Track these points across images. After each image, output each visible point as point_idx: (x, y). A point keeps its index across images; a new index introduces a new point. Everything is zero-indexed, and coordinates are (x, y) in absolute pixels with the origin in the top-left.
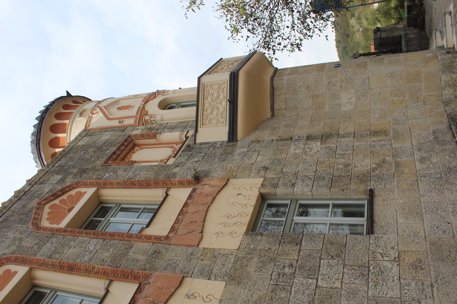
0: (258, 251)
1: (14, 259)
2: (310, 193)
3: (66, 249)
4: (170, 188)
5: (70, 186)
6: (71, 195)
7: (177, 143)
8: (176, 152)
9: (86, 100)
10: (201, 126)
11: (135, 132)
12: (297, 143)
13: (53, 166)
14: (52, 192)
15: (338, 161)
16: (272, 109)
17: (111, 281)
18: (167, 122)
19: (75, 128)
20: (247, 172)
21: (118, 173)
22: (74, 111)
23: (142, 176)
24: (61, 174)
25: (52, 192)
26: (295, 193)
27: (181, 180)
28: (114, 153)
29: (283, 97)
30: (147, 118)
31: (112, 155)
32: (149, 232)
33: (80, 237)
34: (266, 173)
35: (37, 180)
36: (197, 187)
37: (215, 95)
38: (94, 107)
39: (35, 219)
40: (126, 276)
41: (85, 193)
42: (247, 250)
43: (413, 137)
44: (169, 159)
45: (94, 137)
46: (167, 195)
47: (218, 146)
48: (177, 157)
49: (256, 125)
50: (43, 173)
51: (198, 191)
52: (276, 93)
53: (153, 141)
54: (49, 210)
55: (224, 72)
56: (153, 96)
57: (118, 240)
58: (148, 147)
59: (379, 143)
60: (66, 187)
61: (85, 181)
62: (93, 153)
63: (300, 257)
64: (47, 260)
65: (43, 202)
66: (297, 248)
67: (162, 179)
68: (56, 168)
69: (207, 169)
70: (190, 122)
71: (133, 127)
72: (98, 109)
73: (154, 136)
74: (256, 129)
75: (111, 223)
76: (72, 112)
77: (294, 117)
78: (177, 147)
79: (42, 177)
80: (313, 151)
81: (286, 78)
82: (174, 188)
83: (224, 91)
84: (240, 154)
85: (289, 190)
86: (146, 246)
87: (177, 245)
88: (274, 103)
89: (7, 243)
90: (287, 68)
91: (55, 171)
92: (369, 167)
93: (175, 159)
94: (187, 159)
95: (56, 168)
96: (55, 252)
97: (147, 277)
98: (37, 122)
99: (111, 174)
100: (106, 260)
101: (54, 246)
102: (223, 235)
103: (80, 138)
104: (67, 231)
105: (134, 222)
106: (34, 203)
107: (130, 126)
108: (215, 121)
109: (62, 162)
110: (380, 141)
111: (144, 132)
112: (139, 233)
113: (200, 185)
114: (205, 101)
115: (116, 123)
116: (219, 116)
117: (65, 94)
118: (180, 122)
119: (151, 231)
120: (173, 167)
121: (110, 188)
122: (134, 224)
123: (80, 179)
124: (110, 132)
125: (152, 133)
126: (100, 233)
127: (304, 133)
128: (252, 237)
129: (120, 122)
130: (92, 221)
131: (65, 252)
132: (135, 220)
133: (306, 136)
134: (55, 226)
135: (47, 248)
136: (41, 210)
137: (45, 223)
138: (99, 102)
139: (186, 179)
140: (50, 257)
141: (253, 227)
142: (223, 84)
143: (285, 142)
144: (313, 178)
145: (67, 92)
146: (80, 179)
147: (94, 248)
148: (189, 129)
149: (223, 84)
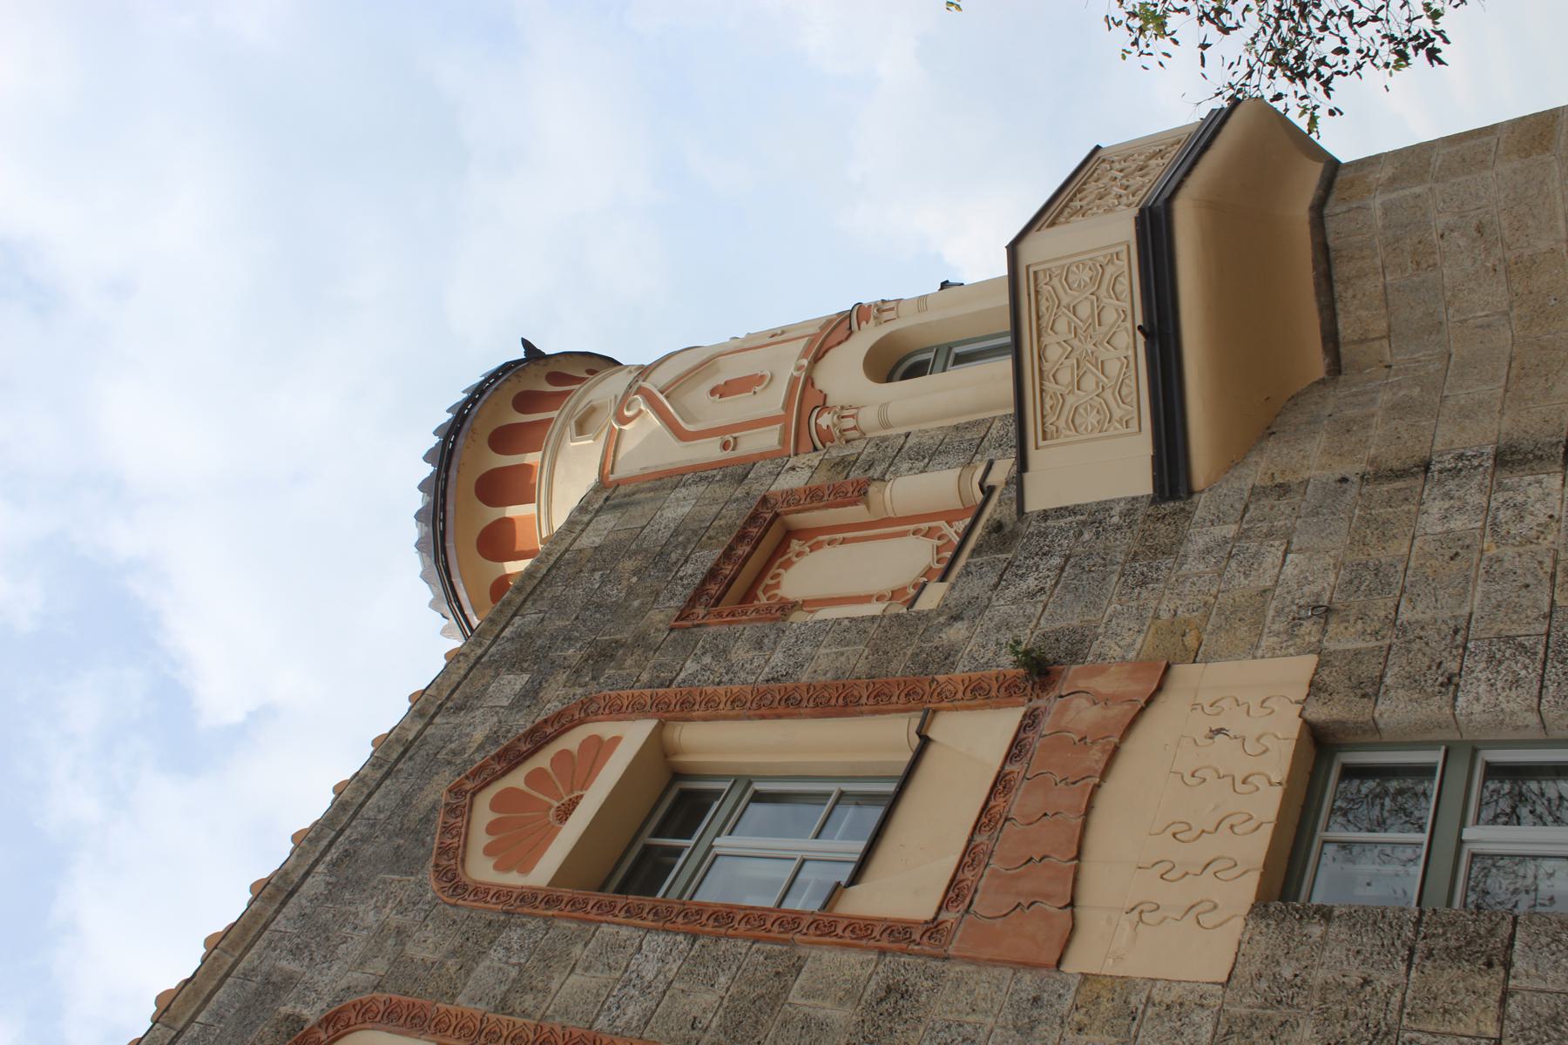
0: (1317, 994)
1: (382, 1008)
2: (1533, 719)
3: (556, 975)
4: (935, 711)
5: (559, 715)
6: (565, 753)
7: (950, 516)
8: (948, 554)
9: (599, 364)
10: (1041, 443)
12: (1451, 485)
13: (497, 637)
14: (496, 742)
16: (1331, 339)
18: (903, 430)
19: (566, 478)
20: (1243, 631)
21: (733, 657)
22: (554, 414)
23: (823, 664)
24: (523, 671)
25: (496, 742)
26: (1461, 719)
27: (975, 675)
28: (712, 574)
30: (826, 420)
31: (703, 582)
32: (863, 902)
33: (604, 928)
34: (1324, 631)
35: (445, 694)
36: (1041, 703)
37: (1084, 310)
38: (626, 394)
39: (444, 850)
41: (616, 740)
42: (1264, 985)
44: (924, 585)
45: (635, 511)
46: (925, 741)
47: (1116, 519)
48: (952, 577)
49: (1265, 417)
50: (463, 667)
51: (1046, 725)
52: (1341, 270)
54: (493, 816)
55: (1110, 210)
56: (843, 326)
57: (746, 939)
58: (840, 536)
60: (546, 721)
61: (613, 694)
62: (634, 579)
63: (1510, 1028)
64: (493, 1017)
65: (469, 785)
66: (1488, 981)
67: (901, 674)
68: (509, 647)
69: (1076, 623)
70: (997, 424)
71: (777, 460)
72: (640, 403)
74: (1269, 432)
75: (720, 859)
76: (550, 420)
77: (1431, 368)
78: (952, 533)
79: (459, 684)
80: (1528, 519)
81: (1378, 201)
82: (949, 709)
83: (1118, 288)
84: (1208, 551)
85: (1435, 708)
87: (973, 961)
88: (1334, 316)
89: (357, 945)
90: (1378, 157)
91: (503, 656)
93: (945, 586)
94: (996, 586)
95: (509, 647)
96: (521, 986)
98: (428, 469)
99: (707, 660)
100: (705, 1022)
101: (514, 960)
102: (1158, 915)
103: (586, 518)
104: (559, 900)
105: (807, 855)
106: (437, 790)
107: (763, 456)
108: (1093, 418)
109: (528, 619)
111: (820, 479)
112: (824, 907)
113: (1052, 695)
114: (1046, 340)
115: (709, 451)
116: (1108, 394)
117: (519, 354)
118: (957, 428)
119: (875, 899)
120: (942, 619)
121: (705, 719)
122: (804, 861)
123: (593, 688)
124: (693, 488)
126: (677, 908)
127: (1482, 435)
128: (1286, 924)
129: (725, 446)
130: (647, 849)
131: (554, 986)
132: (806, 845)
133: (1490, 450)
134: (513, 879)
135: (493, 969)
136: (462, 815)
137: (481, 869)
138: (644, 371)
139: (995, 670)
140: (503, 1006)
141: (1284, 883)
142: (1111, 261)
143: (1399, 484)
144: (1540, 649)
145: (525, 343)
146: (593, 688)
147: (659, 972)
148: (992, 454)
149: (1111, 261)
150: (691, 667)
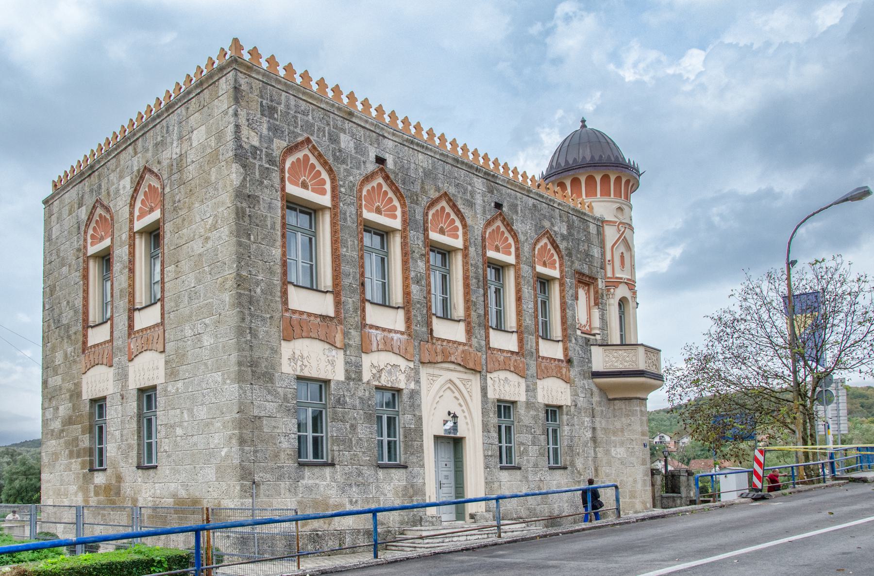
11: (600, 281)
16: (615, 399)
17: (517, 332)
23: (569, 313)
29: (623, 407)
40: (521, 341)
53: (592, 303)
73: (596, 304)
85: (565, 423)
86: (534, 345)
97: (523, 355)
111: (600, 291)
115: (608, 257)
125: (598, 301)
127: (597, 425)
150: (568, 280)
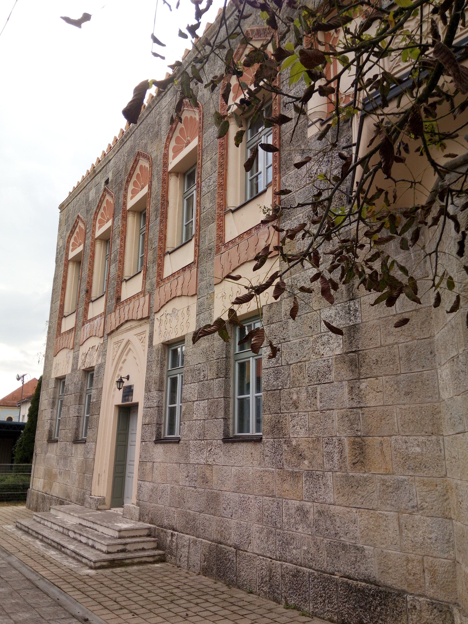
15: (303, 390)
34: (287, 298)
43: (348, 510)
59: (337, 450)
80: (322, 347)
92: (292, 436)
110: (341, 452)
133: (359, 321)
143: (345, 292)
144: (278, 365)
